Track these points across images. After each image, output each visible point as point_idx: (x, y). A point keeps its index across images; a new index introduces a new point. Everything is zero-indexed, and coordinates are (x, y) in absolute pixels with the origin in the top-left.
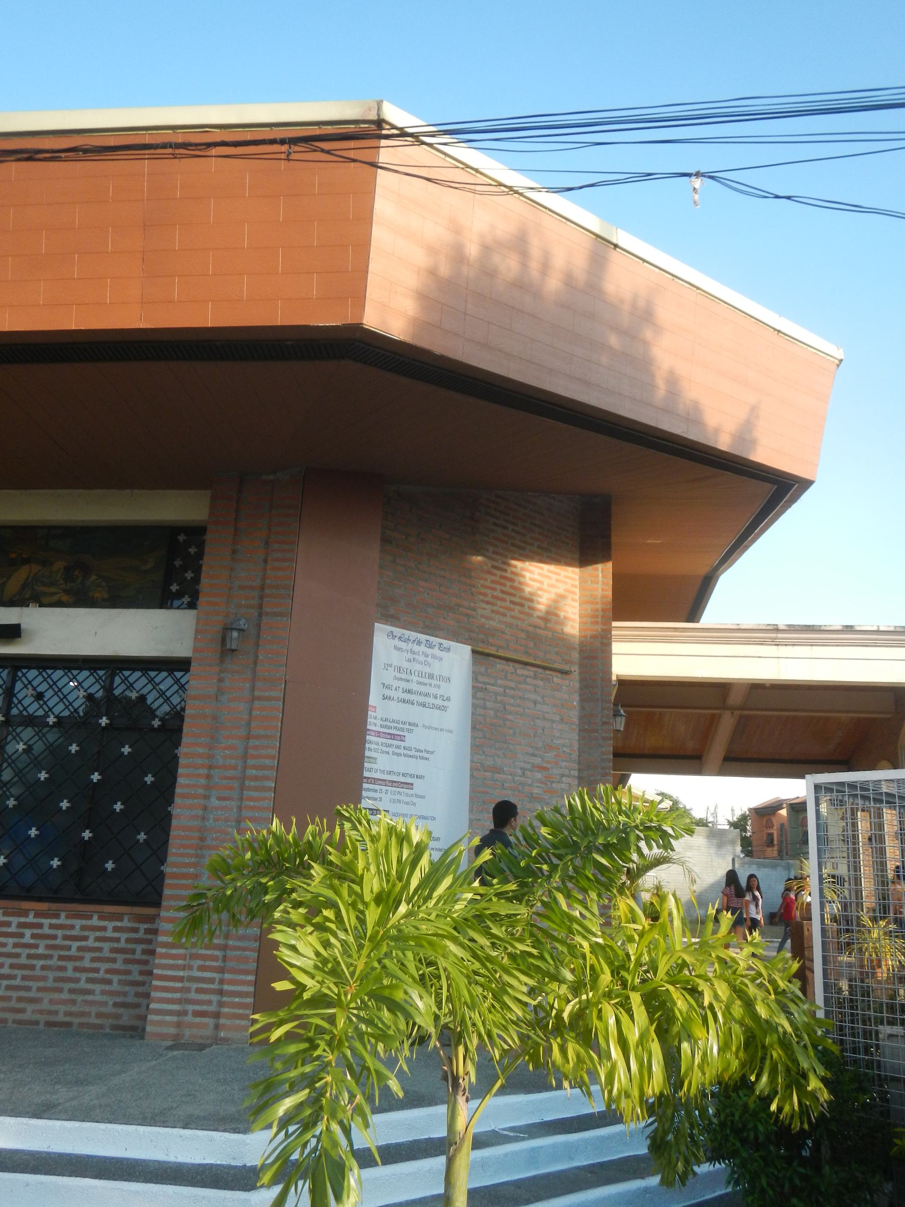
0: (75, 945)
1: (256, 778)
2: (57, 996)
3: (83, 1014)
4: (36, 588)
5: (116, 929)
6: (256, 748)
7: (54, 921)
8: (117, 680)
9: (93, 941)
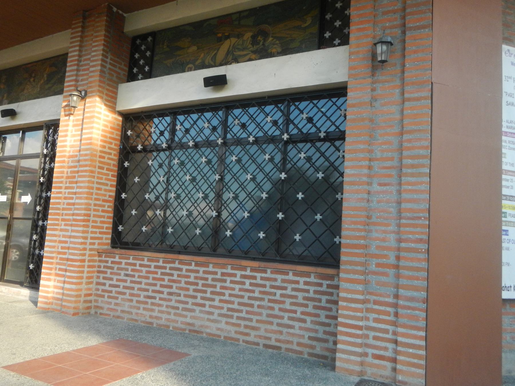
0: (279, 292)
1: (413, 166)
2: (269, 327)
3: (288, 342)
4: (235, 53)
5: (306, 283)
6: (409, 141)
7: (264, 275)
8: (292, 108)
9: (290, 290)
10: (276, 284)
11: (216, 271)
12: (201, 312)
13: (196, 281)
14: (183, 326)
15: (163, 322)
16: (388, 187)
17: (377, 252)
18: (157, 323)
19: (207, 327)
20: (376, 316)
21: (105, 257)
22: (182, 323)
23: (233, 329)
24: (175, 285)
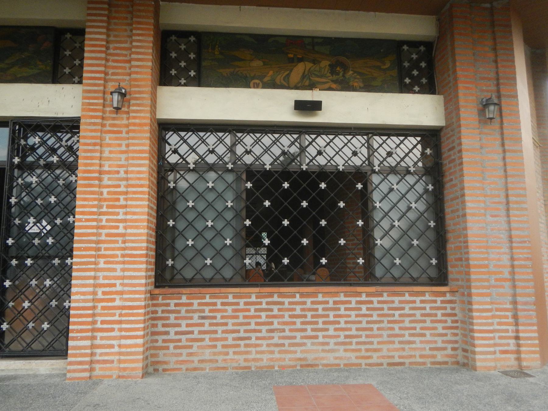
0: (397, 313)
2: (391, 346)
3: (411, 356)
4: (311, 78)
5: (422, 302)
6: (513, 183)
7: (380, 299)
9: (408, 310)
10: (394, 306)
11: (327, 300)
12: (313, 344)
13: (303, 313)
14: (292, 363)
15: (265, 363)
16: (498, 218)
17: (494, 270)
18: (255, 366)
19: (323, 358)
20: (498, 320)
21: (163, 299)
22: (290, 360)
23: (352, 355)
24: (276, 321)
